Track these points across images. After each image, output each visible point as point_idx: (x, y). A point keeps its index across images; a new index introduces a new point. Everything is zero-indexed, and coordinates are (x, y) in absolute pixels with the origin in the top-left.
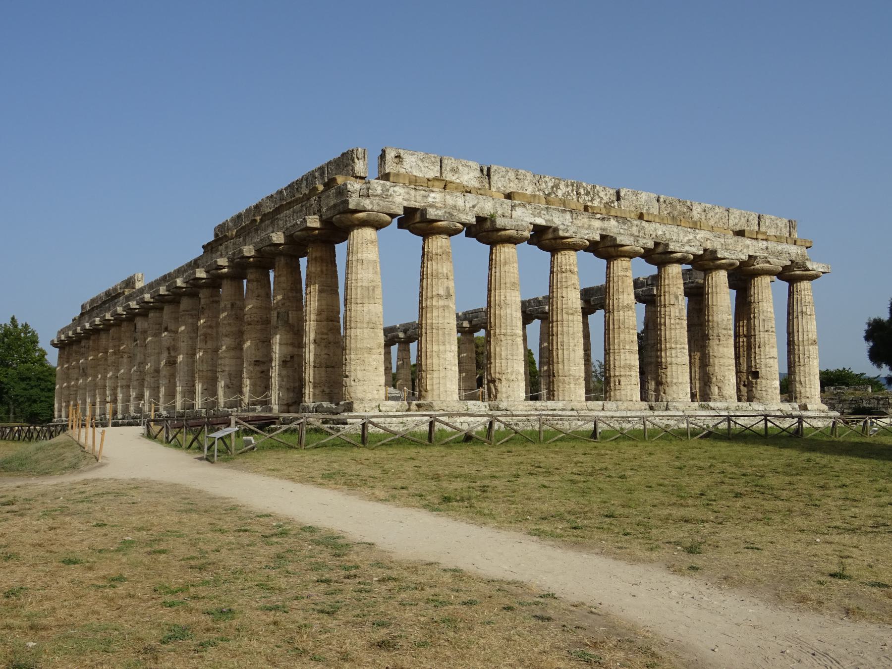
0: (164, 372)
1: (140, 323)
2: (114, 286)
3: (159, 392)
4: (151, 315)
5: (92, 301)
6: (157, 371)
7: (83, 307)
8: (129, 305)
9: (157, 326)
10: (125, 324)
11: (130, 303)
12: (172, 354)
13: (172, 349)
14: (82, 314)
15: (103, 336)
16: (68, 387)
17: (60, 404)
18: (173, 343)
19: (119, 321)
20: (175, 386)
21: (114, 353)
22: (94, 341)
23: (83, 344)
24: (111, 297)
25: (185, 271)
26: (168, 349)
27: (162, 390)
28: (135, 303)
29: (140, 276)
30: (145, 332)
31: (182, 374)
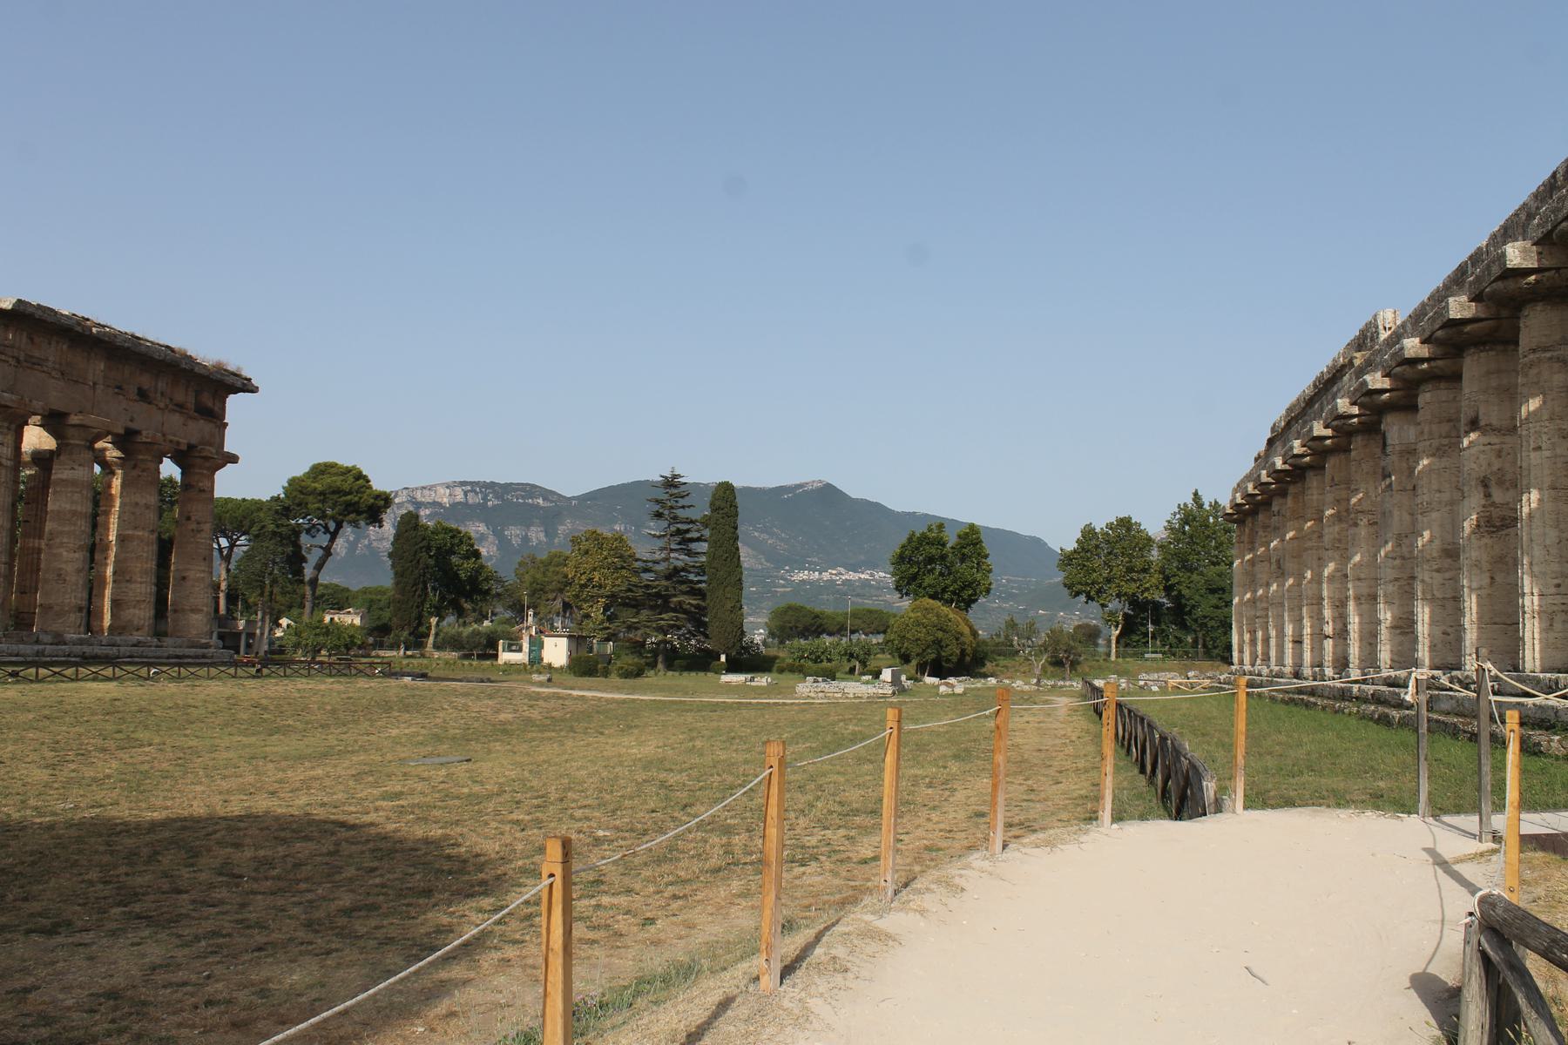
0: (1475, 552)
1: (1396, 430)
2: (1330, 362)
3: (1460, 612)
4: (1425, 397)
5: (1290, 410)
6: (1452, 553)
7: (1273, 429)
8: (1365, 383)
9: (1445, 427)
10: (1357, 442)
11: (1367, 378)
12: (1498, 496)
13: (1503, 482)
14: (1271, 442)
15: (1313, 481)
16: (1253, 601)
17: (1241, 635)
18: (1496, 465)
19: (1344, 431)
20: (1514, 592)
21: (1338, 518)
22: (1296, 497)
23: (1275, 508)
24: (1327, 385)
25: (1530, 216)
26: (1485, 483)
27: (1471, 604)
28: (1378, 375)
29: (1389, 315)
30: (1411, 453)
31: (1538, 552)
